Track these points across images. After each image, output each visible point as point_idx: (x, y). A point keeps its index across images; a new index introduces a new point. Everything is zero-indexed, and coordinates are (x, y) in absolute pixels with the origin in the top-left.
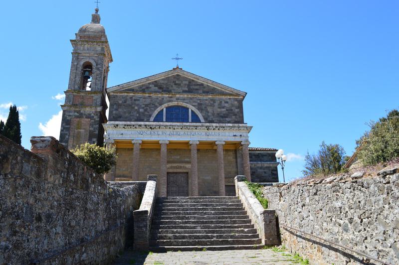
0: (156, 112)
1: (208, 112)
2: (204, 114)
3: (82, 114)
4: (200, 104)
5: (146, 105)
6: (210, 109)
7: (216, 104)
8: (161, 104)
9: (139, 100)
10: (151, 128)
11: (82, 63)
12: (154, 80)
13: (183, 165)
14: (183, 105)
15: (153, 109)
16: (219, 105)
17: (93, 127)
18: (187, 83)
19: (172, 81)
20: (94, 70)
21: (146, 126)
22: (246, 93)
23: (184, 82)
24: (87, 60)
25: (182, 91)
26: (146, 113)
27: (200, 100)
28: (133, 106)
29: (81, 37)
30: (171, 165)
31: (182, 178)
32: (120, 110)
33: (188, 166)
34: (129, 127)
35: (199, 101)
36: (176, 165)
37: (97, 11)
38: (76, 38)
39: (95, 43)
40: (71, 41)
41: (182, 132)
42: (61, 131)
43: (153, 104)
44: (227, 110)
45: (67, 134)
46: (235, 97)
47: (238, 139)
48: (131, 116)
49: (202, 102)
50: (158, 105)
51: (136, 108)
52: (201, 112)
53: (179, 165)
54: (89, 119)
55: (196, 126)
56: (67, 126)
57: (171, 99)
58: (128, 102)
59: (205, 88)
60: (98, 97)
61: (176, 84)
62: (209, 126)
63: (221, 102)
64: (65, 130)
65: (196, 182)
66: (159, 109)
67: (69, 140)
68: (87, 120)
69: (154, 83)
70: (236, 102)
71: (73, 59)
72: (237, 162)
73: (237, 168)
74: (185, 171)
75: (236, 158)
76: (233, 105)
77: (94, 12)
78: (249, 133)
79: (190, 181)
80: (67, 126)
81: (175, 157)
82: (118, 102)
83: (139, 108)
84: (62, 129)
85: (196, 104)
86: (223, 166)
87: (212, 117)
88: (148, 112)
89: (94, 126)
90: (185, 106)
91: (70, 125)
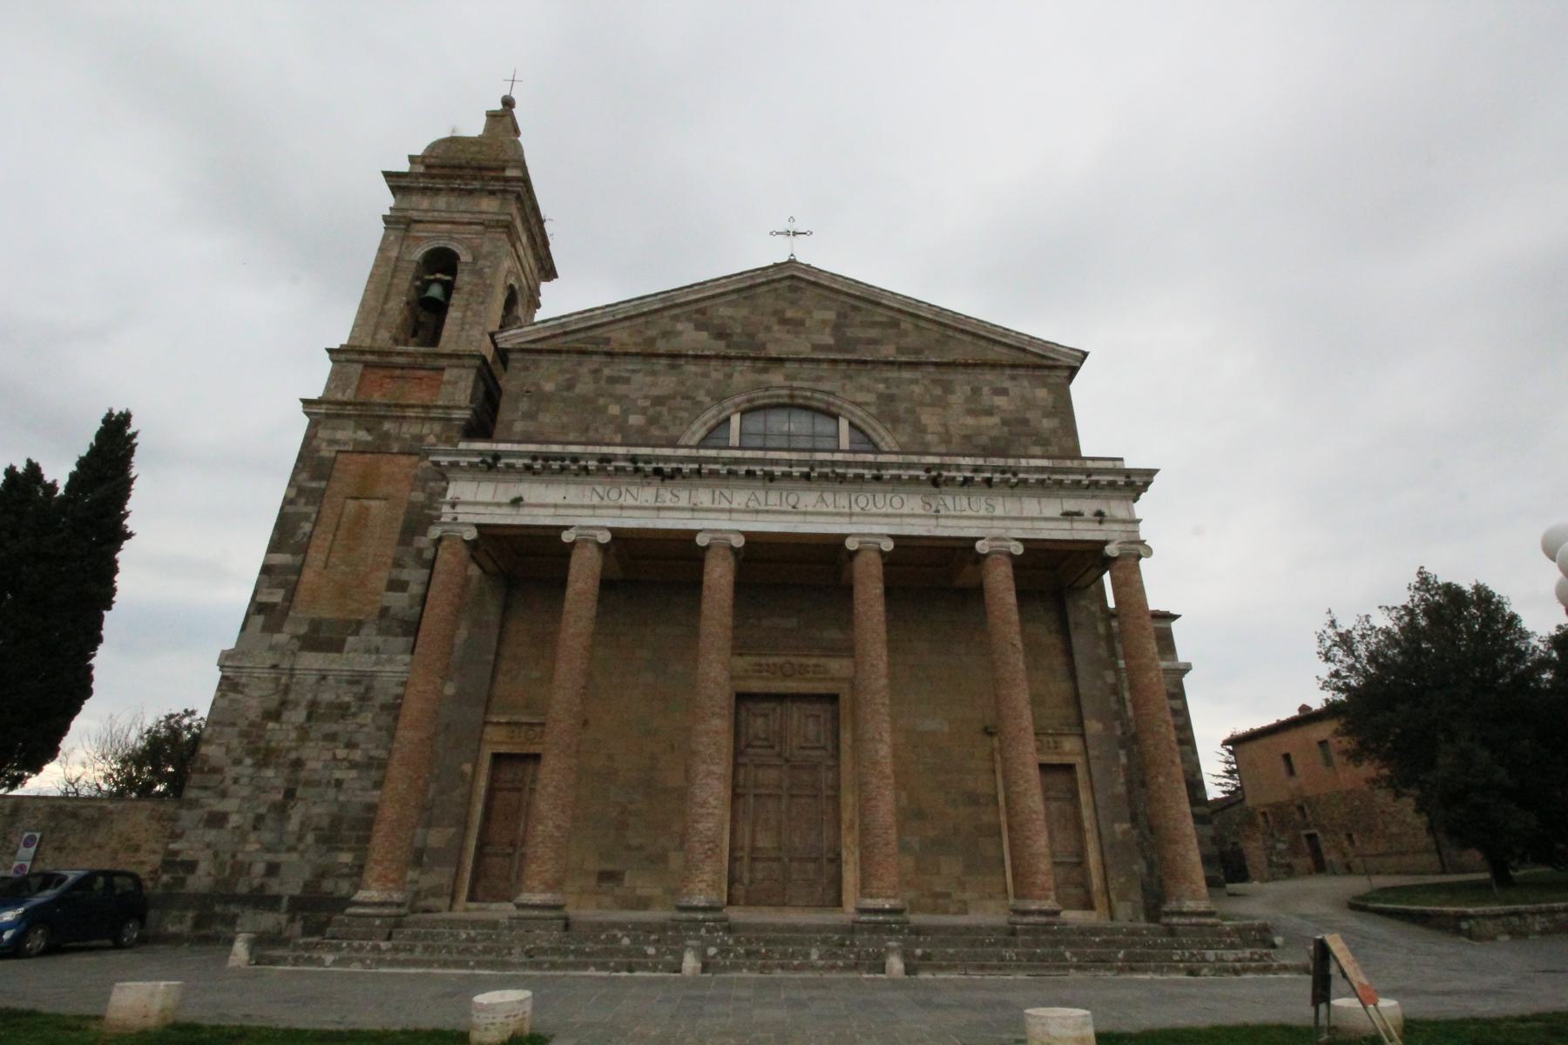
0: (698, 431)
1: (921, 429)
2: (904, 439)
3: (386, 436)
4: (887, 399)
5: (658, 401)
6: (929, 419)
7: (957, 398)
8: (719, 399)
9: (627, 381)
10: (658, 472)
11: (418, 253)
12: (694, 307)
13: (814, 661)
14: (815, 404)
15: (685, 415)
16: (968, 400)
18: (831, 315)
20: (464, 279)
21: (634, 459)
22: (1085, 354)
23: (819, 315)
24: (441, 243)
25: (809, 346)
26: (655, 432)
27: (885, 381)
29: (428, 167)
31: (811, 723)
32: (546, 418)
33: (838, 666)
34: (556, 465)
35: (881, 387)
37: (508, 103)
38: (411, 168)
39: (477, 185)
40: (388, 175)
41: (808, 499)
42: (287, 501)
44: (1005, 422)
45: (306, 517)
46: (1038, 373)
47: (1085, 531)
49: (894, 391)
50: (707, 400)
51: (614, 410)
52: (892, 432)
54: (415, 459)
55: (880, 466)
56: (314, 485)
57: (764, 377)
58: (581, 388)
59: (905, 334)
60: (463, 372)
61: (784, 321)
62: (942, 466)
63: (976, 391)
64: (303, 500)
65: (884, 750)
66: (710, 417)
67: (315, 542)
68: (404, 460)
69: (695, 316)
70: (1042, 393)
71: (385, 238)
72: (1069, 652)
73: (1072, 674)
74: (821, 688)
75: (1064, 630)
76: (1029, 404)
77: (498, 106)
78: (1135, 501)
79: (846, 736)
80: (314, 485)
82: (537, 385)
83: (625, 412)
84: (293, 493)
85: (871, 398)
86: (1021, 665)
88: (665, 428)
89: (432, 484)
90: (822, 406)
91: (328, 478)
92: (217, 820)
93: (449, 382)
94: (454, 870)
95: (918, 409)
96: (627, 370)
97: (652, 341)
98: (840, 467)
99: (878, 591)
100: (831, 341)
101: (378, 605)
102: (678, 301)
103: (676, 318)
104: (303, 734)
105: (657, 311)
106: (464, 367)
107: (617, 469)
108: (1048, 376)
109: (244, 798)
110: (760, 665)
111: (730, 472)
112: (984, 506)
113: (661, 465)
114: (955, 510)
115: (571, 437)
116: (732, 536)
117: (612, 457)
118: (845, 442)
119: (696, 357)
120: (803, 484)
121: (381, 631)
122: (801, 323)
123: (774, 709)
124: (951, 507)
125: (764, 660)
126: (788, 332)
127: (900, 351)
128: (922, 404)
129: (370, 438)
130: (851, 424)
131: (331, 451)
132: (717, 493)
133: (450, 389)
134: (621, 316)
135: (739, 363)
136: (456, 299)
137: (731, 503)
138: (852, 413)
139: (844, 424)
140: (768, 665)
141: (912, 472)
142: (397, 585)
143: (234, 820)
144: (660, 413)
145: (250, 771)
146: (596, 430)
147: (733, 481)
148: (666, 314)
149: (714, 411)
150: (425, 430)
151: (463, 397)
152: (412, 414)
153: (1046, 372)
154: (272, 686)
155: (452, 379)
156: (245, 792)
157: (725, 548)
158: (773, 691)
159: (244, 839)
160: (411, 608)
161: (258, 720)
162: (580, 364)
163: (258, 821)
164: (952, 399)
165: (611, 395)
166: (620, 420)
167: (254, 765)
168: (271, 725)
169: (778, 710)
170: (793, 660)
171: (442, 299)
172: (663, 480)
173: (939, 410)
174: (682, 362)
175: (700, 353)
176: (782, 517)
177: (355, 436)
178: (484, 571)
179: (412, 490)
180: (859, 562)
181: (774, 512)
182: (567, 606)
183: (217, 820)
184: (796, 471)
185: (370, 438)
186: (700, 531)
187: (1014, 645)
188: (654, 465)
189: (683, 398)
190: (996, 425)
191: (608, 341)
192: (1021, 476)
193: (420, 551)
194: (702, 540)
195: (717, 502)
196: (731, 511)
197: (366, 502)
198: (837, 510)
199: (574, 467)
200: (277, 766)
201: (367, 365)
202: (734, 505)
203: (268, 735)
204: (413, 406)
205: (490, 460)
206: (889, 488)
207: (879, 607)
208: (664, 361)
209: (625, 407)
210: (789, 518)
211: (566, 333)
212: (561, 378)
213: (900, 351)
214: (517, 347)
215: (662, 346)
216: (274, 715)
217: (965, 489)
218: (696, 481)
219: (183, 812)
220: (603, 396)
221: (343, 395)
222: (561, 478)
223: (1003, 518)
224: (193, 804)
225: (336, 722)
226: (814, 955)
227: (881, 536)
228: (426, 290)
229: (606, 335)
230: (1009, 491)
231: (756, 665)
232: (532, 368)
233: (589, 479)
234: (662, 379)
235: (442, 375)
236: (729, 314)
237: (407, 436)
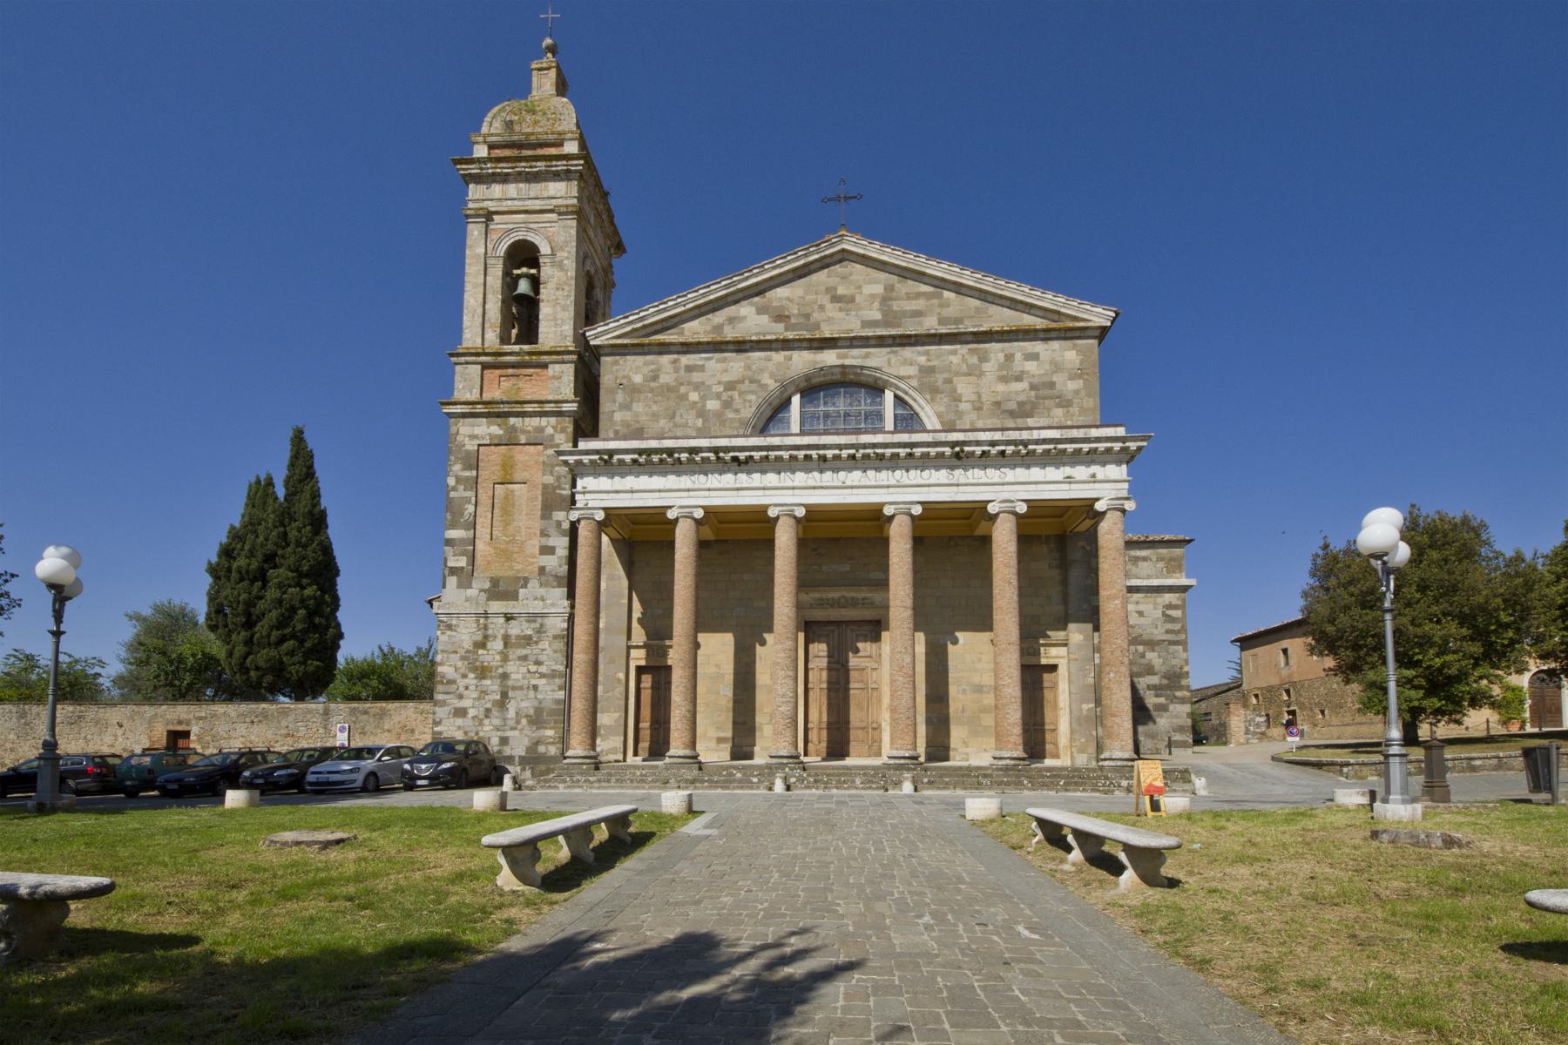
2: (942, 409)
5: (730, 386)
6: (964, 388)
17: (552, 473)
19: (824, 288)
25: (859, 323)
26: (730, 415)
28: (683, 390)
30: (817, 595)
32: (638, 407)
35: (922, 360)
43: (751, 382)
48: (676, 425)
49: (935, 363)
51: (694, 396)
54: (541, 447)
56: (467, 474)
61: (836, 299)
80: (467, 474)
82: (628, 378)
83: (704, 398)
85: (912, 371)
87: (974, 416)
88: (737, 411)
89: (557, 468)
92: (461, 713)
93: (554, 377)
94: (622, 738)
95: (955, 379)
100: (878, 316)
104: (505, 659)
106: (563, 362)
109: (474, 699)
110: (822, 600)
121: (541, 585)
122: (852, 300)
123: (833, 631)
126: (841, 310)
127: (942, 321)
128: (958, 374)
129: (501, 432)
130: (896, 396)
131: (473, 445)
133: (556, 383)
136: (544, 293)
138: (898, 388)
139: (889, 396)
140: (828, 600)
142: (548, 550)
143: (472, 712)
145: (475, 681)
146: (681, 416)
151: (567, 391)
154: (475, 625)
156: (475, 695)
158: (832, 619)
159: (481, 724)
160: (560, 566)
161: (471, 648)
163: (488, 712)
164: (986, 367)
165: (689, 383)
167: (476, 678)
168: (481, 652)
169: (836, 632)
173: (973, 379)
175: (762, 338)
177: (489, 431)
178: (611, 539)
179: (544, 475)
183: (461, 713)
185: (501, 432)
189: (751, 382)
193: (559, 523)
197: (510, 486)
200: (491, 678)
201: (485, 366)
203: (481, 658)
209: (702, 393)
212: (646, 370)
213: (942, 321)
216: (482, 645)
219: (437, 709)
220: (682, 384)
224: (443, 703)
225: (524, 648)
226: (858, 781)
231: (818, 599)
234: (731, 364)
236: (786, 295)
237: (530, 428)
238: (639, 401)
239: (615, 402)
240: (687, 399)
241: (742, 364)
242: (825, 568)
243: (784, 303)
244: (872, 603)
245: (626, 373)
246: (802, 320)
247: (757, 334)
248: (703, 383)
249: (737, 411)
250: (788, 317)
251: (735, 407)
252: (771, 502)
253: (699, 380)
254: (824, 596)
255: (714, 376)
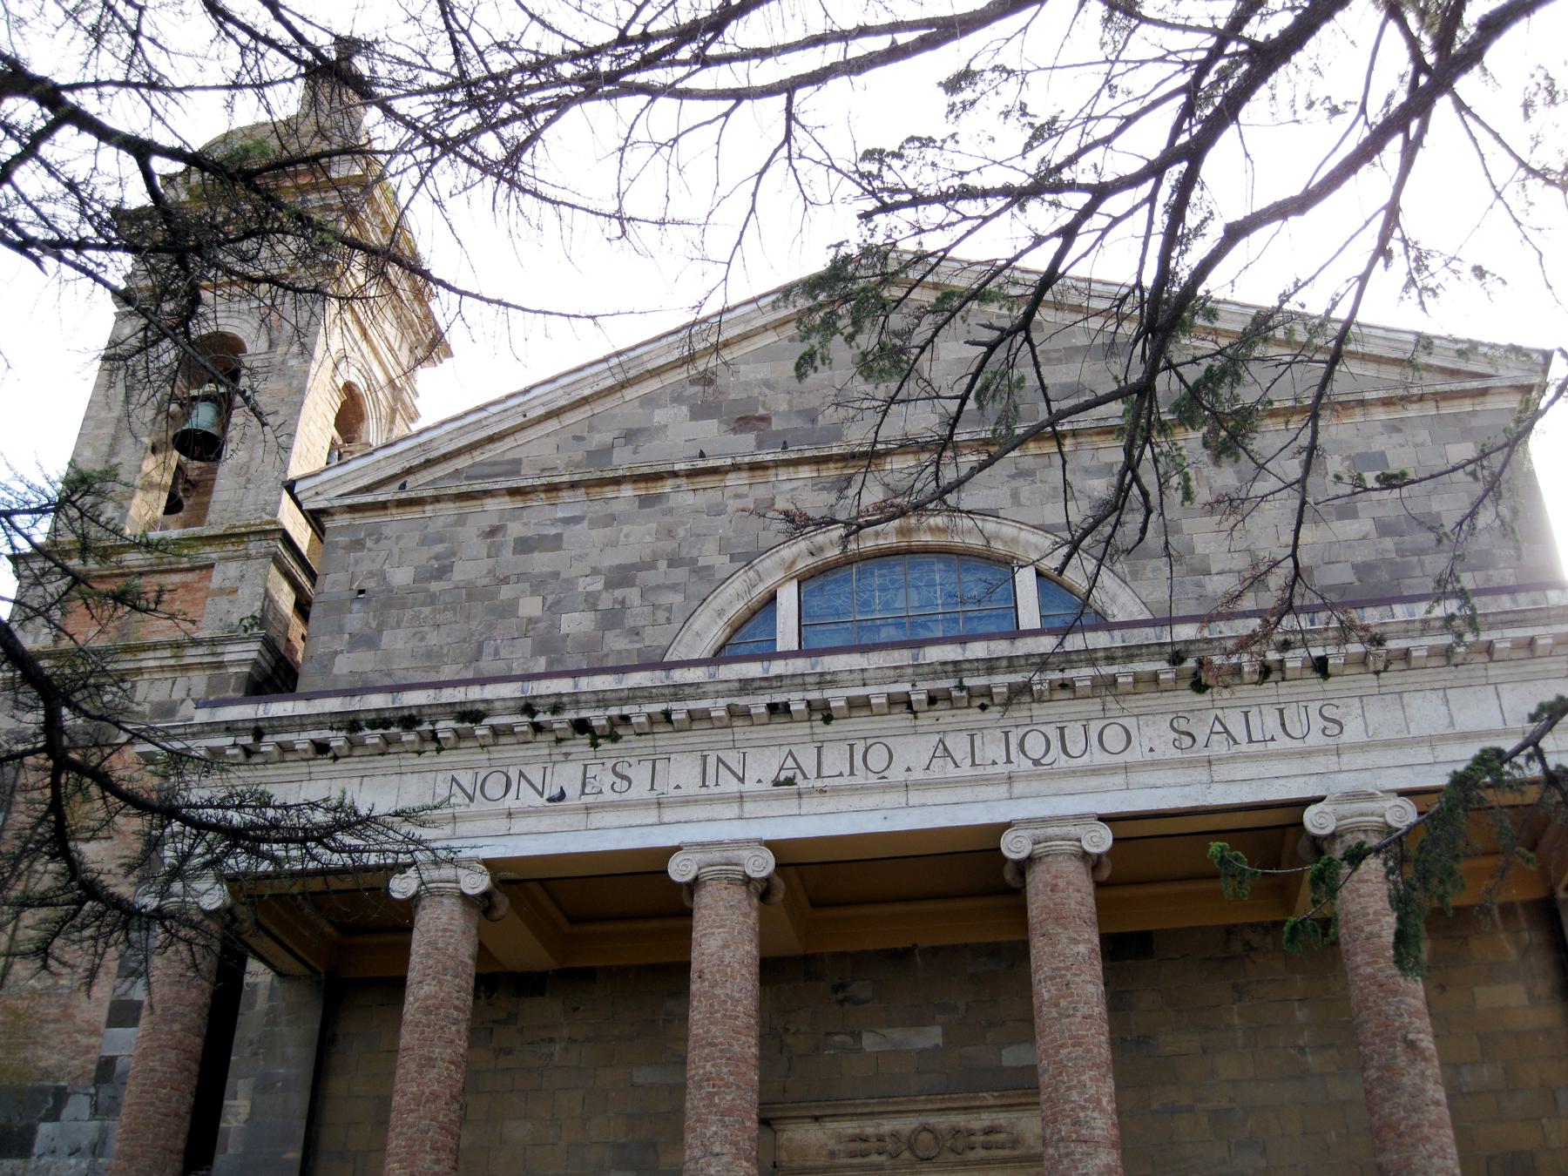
0: (707, 632)
5: (621, 577)
8: (748, 559)
9: (555, 543)
10: (581, 726)
15: (677, 599)
21: (528, 709)
30: (849, 1127)
32: (396, 641)
34: (372, 737)
36: (905, 1124)
43: (673, 563)
46: (1448, 408)
50: (721, 562)
51: (531, 607)
53: (942, 1122)
66: (733, 599)
81: (896, 1034)
82: (382, 576)
90: (975, 542)
93: (221, 591)
96: (555, 522)
97: (603, 454)
98: (976, 672)
99: (1082, 948)
101: (93, 1056)
102: (650, 366)
103: (648, 401)
105: (610, 391)
106: (248, 557)
107: (496, 732)
108: (1474, 413)
110: (865, 1140)
111: (732, 711)
112: (1317, 723)
113: (584, 714)
114: (1250, 741)
115: (447, 673)
116: (745, 854)
117: (481, 707)
118: (1029, 616)
119: (693, 474)
120: (900, 719)
124: (1238, 731)
125: (870, 1128)
132: (712, 760)
134: (541, 411)
135: (783, 474)
137: (742, 780)
139: (1026, 581)
140: (881, 1139)
141: (1142, 667)
144: (623, 602)
146: (496, 652)
147: (741, 731)
148: (630, 393)
149: (737, 584)
150: (178, 694)
152: (152, 663)
153: (1466, 406)
155: (227, 584)
157: (731, 881)
162: (461, 520)
165: (521, 577)
166: (542, 625)
170: (933, 1120)
171: (213, 431)
172: (595, 745)
174: (667, 486)
176: (856, 802)
178: (280, 974)
180: (1036, 881)
181: (837, 791)
182: (407, 1037)
184: (877, 693)
186: (677, 849)
187: (1411, 1045)
188: (571, 715)
190: (1364, 538)
191: (514, 467)
192: (1392, 645)
194: (680, 869)
195: (711, 781)
196: (741, 798)
198: (980, 771)
199: (409, 737)
202: (750, 785)
204: (155, 647)
205: (248, 740)
206: (1094, 706)
207: (1089, 986)
208: (627, 491)
209: (550, 599)
210: (871, 801)
211: (429, 463)
212: (423, 556)
214: (337, 503)
215: (624, 460)
217: (1269, 688)
218: (664, 739)
220: (505, 580)
221: (35, 641)
222: (388, 762)
223: (1363, 747)
227: (1080, 818)
228: (187, 416)
229: (509, 456)
230: (1369, 681)
231: (853, 1139)
232: (369, 544)
233: (445, 757)
234: (626, 528)
235: (209, 578)
236: (760, 376)
237: (147, 708)
238: (399, 625)
239: (341, 630)
240: (515, 614)
241: (654, 526)
242: (869, 1042)
243: (756, 392)
244: (1015, 1143)
245: (376, 567)
246: (797, 423)
247: (690, 459)
248: (556, 575)
249: (636, 632)
250: (765, 419)
251: (630, 622)
252: (675, 843)
253: (545, 569)
254: (870, 1128)
255: (581, 557)
